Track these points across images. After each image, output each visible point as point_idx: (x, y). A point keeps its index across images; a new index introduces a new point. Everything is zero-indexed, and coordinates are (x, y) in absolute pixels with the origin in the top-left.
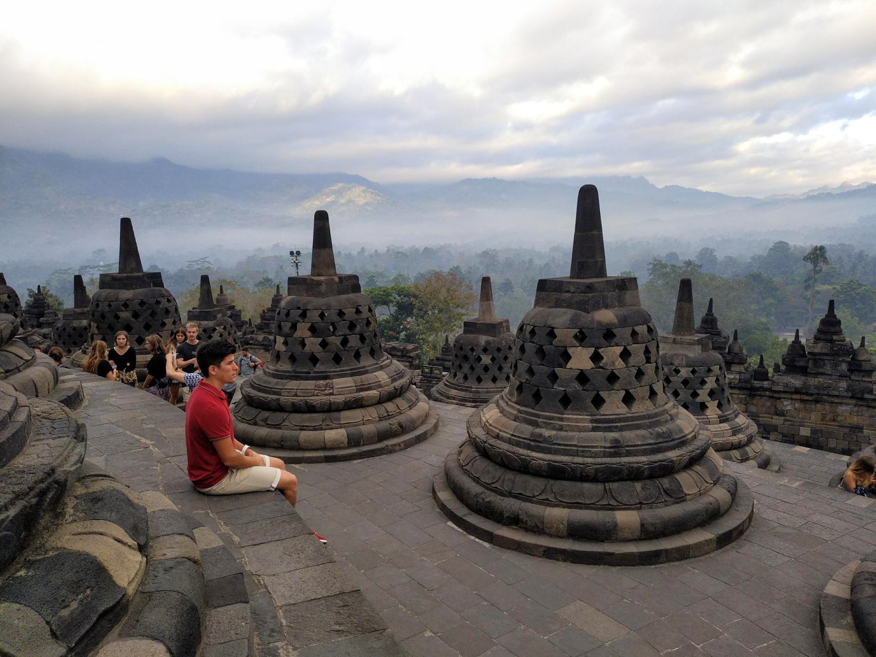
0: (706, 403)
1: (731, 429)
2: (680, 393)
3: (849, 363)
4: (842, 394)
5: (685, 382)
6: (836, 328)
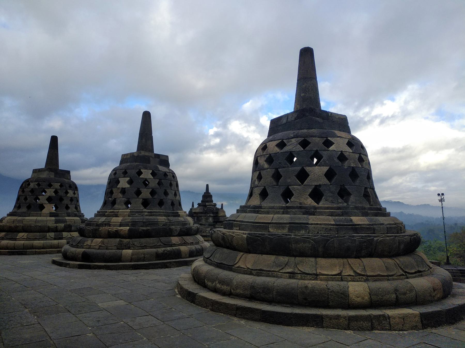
0: (44, 205)
1: (55, 220)
2: (28, 198)
3: (214, 217)
4: (208, 235)
5: (32, 191)
6: (208, 199)
